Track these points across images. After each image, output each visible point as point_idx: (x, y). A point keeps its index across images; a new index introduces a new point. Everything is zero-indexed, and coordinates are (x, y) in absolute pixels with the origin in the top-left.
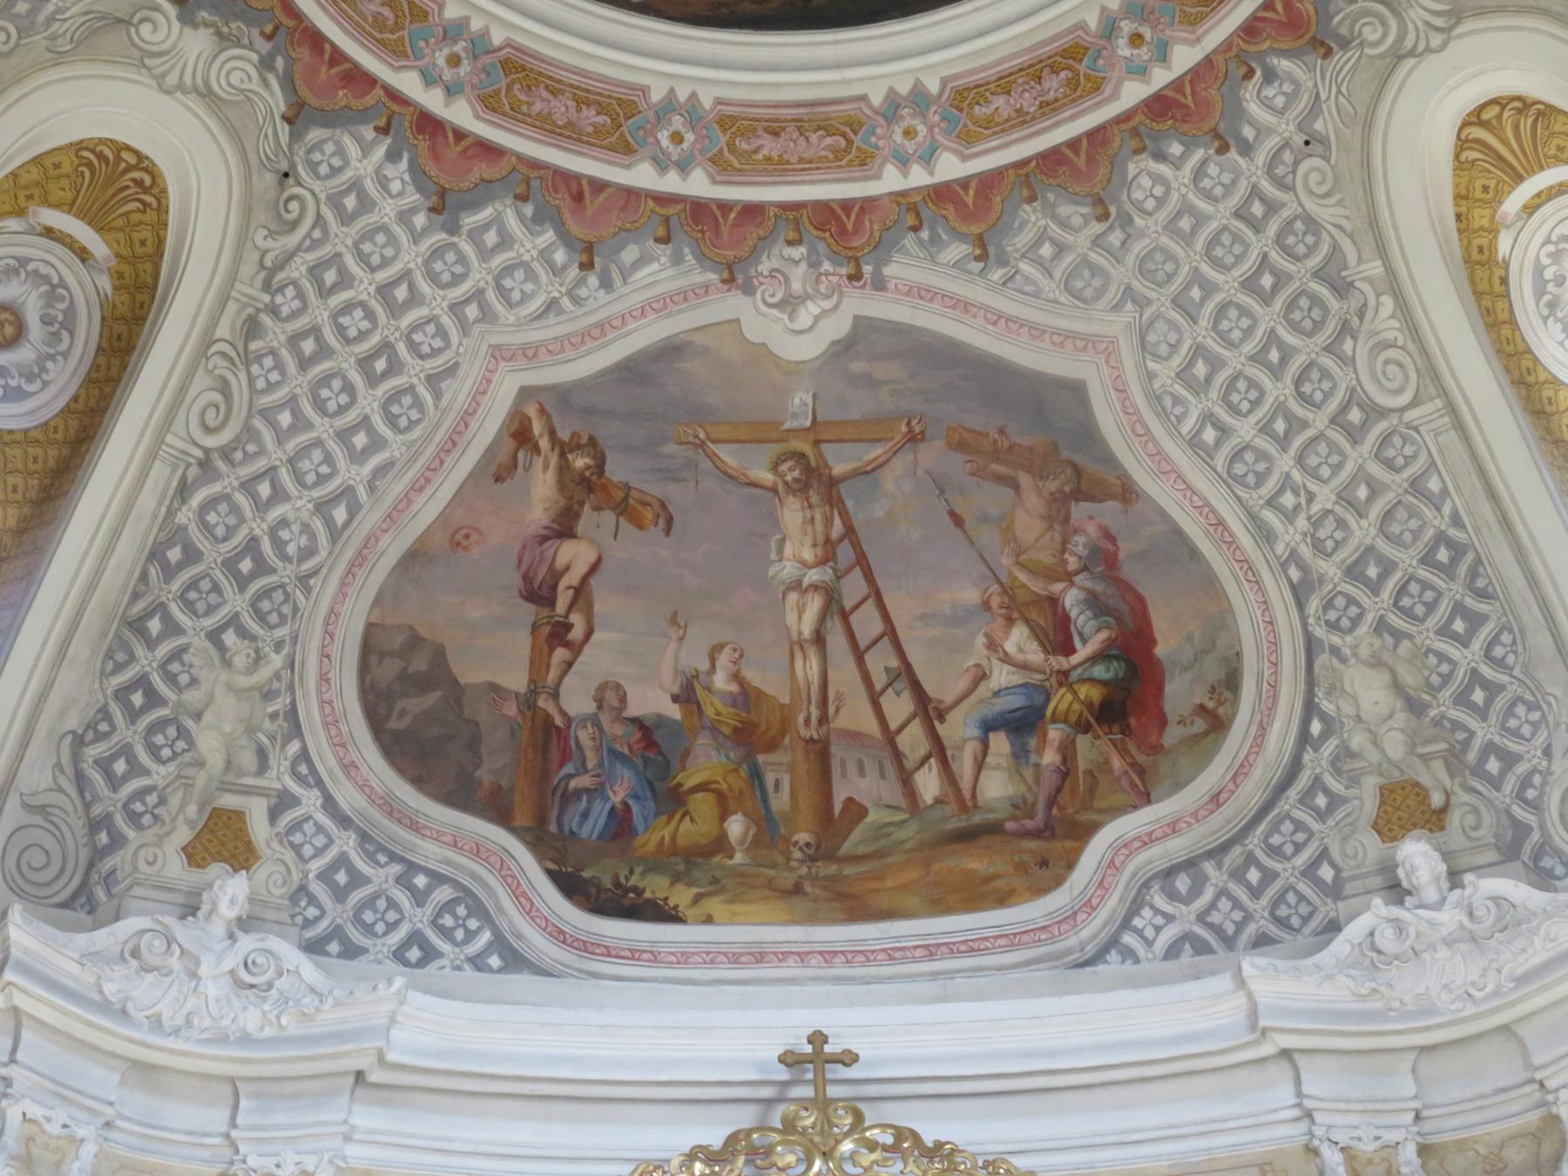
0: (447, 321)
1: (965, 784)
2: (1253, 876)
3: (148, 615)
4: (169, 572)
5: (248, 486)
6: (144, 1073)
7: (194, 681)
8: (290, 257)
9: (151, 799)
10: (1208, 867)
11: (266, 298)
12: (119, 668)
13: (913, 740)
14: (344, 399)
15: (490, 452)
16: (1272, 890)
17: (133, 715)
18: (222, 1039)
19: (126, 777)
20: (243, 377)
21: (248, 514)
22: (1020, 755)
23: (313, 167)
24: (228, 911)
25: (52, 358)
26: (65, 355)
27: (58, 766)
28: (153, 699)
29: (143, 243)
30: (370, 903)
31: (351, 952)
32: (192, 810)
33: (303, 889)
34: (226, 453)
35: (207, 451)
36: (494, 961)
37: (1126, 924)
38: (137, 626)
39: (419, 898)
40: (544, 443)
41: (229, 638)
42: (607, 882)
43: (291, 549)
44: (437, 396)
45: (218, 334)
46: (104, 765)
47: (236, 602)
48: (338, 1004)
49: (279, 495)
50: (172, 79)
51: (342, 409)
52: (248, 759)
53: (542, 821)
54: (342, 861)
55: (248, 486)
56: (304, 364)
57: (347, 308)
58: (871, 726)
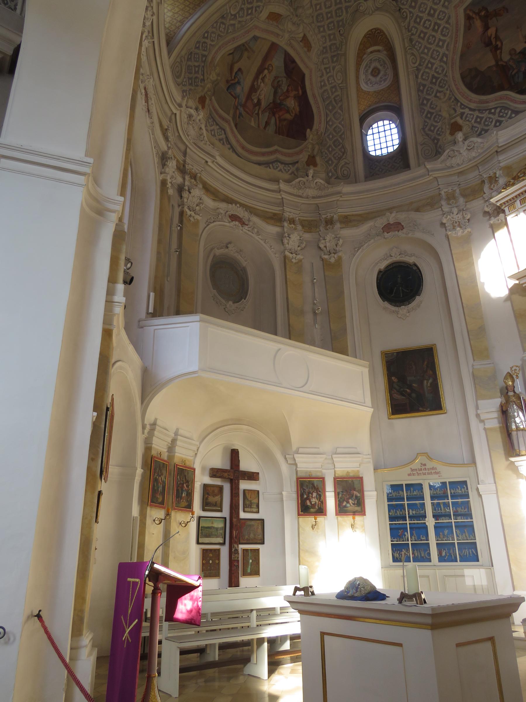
0: (443, 9)
3: (423, 101)
4: (422, 91)
5: (427, 67)
6: (461, 173)
7: (436, 106)
8: (409, 23)
9: (440, 130)
11: (410, 33)
12: (423, 113)
14: (434, 39)
15: (465, 26)
17: (430, 119)
18: (470, 160)
19: (434, 129)
20: (415, 50)
21: (430, 72)
23: (403, 4)
24: (460, 140)
25: (386, 70)
26: (388, 68)
27: (423, 135)
28: (432, 114)
29: (386, 41)
31: (486, 131)
32: (447, 127)
33: (473, 126)
34: (420, 65)
35: (416, 67)
38: (422, 104)
39: (494, 114)
40: (474, 16)
41: (438, 94)
43: (440, 72)
44: (449, 24)
45: (406, 46)
46: (430, 130)
47: (436, 88)
48: (487, 142)
49: (433, 64)
50: (371, 12)
51: (434, 41)
52: (452, 112)
54: (477, 117)
55: (427, 67)
56: (423, 39)
57: (424, 23)
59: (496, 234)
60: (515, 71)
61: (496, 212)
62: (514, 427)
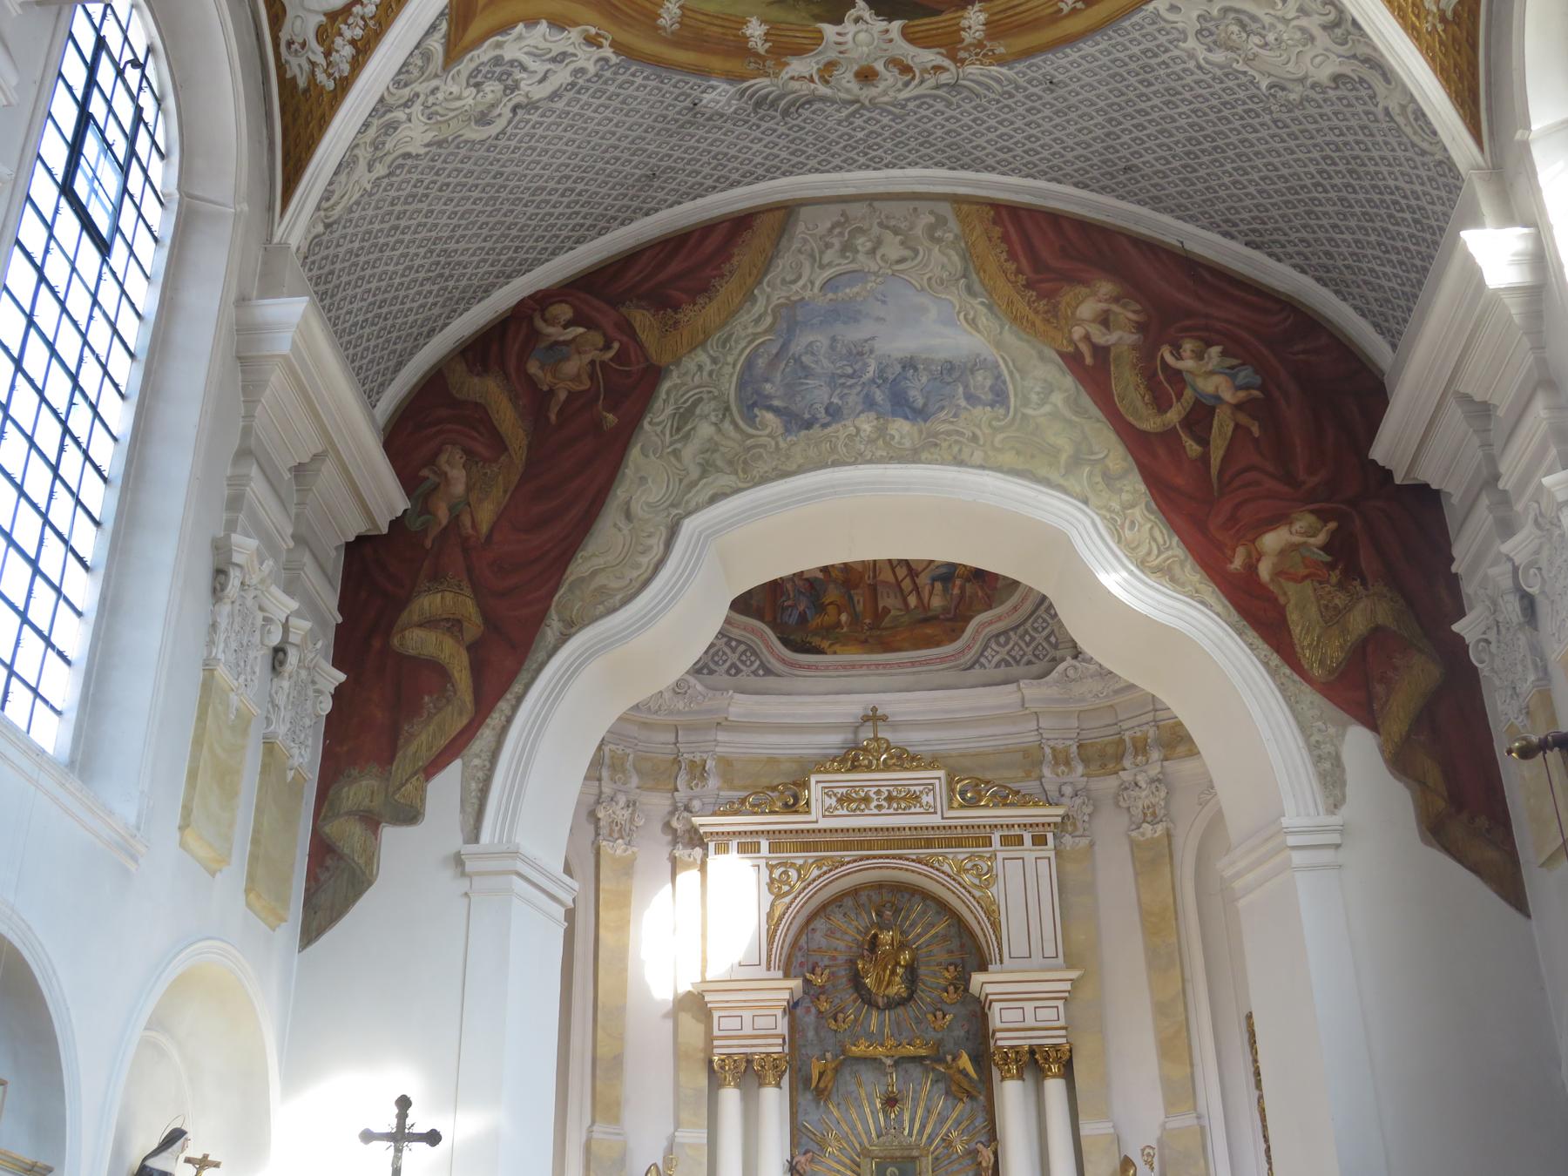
1: (926, 601)
2: (1027, 638)
10: (1011, 633)
13: (907, 584)
16: (1033, 645)
18: (671, 713)
22: (945, 590)
30: (716, 653)
31: (711, 672)
36: (761, 672)
37: (982, 654)
39: (734, 650)
42: (799, 640)
53: (775, 618)
58: (891, 579)
59: (679, 877)
60: (789, 603)
61: (687, 836)
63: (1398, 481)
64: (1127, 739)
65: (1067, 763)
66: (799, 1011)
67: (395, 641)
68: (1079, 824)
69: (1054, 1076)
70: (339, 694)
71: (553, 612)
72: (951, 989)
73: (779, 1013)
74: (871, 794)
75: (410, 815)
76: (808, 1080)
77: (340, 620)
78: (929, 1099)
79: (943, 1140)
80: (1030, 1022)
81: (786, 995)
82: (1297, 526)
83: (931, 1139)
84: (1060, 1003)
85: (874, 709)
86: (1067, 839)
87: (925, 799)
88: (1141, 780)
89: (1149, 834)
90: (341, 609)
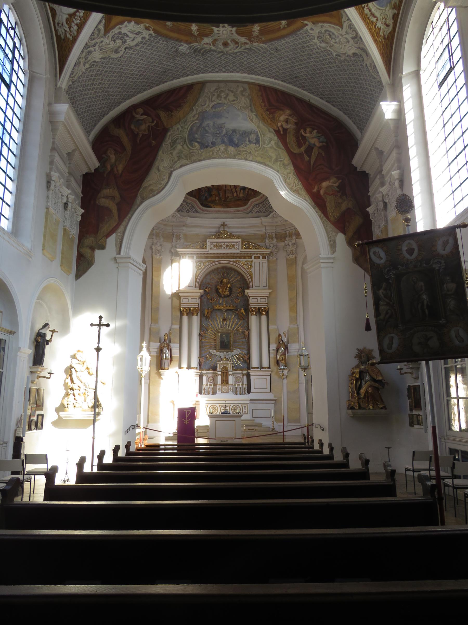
2: (264, 206)
10: (260, 204)
13: (234, 190)
22: (244, 192)
30: (183, 207)
31: (182, 211)
37: (252, 210)
39: (188, 206)
60: (203, 194)
62: (165, 357)
63: (358, 170)
64: (287, 232)
65: (272, 238)
66: (203, 298)
67: (97, 202)
68: (274, 254)
69: (264, 315)
70: (83, 215)
71: (139, 195)
72: (240, 293)
73: (198, 298)
74: (222, 245)
75: (103, 247)
76: (204, 314)
77: (82, 196)
78: (234, 319)
79: (236, 329)
80: (259, 302)
81: (199, 294)
82: (331, 181)
83: (233, 329)
84: (266, 298)
85: (224, 223)
86: (271, 257)
87: (236, 246)
88: (290, 243)
89: (291, 257)
90: (82, 193)
